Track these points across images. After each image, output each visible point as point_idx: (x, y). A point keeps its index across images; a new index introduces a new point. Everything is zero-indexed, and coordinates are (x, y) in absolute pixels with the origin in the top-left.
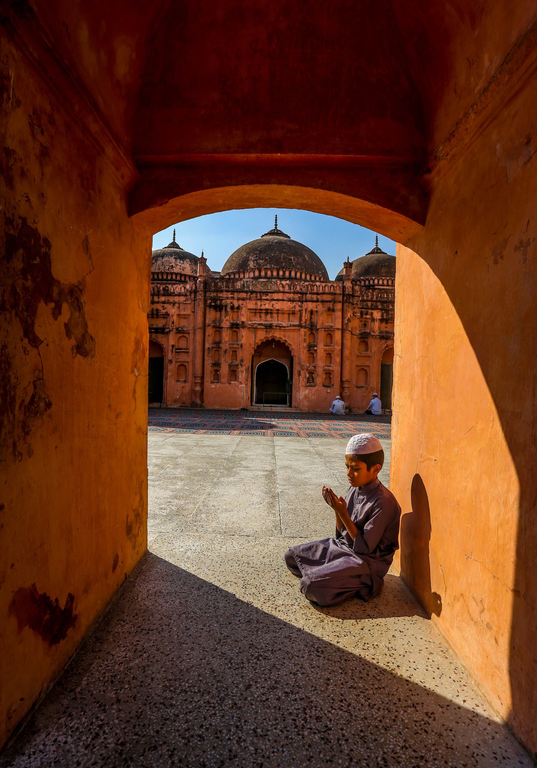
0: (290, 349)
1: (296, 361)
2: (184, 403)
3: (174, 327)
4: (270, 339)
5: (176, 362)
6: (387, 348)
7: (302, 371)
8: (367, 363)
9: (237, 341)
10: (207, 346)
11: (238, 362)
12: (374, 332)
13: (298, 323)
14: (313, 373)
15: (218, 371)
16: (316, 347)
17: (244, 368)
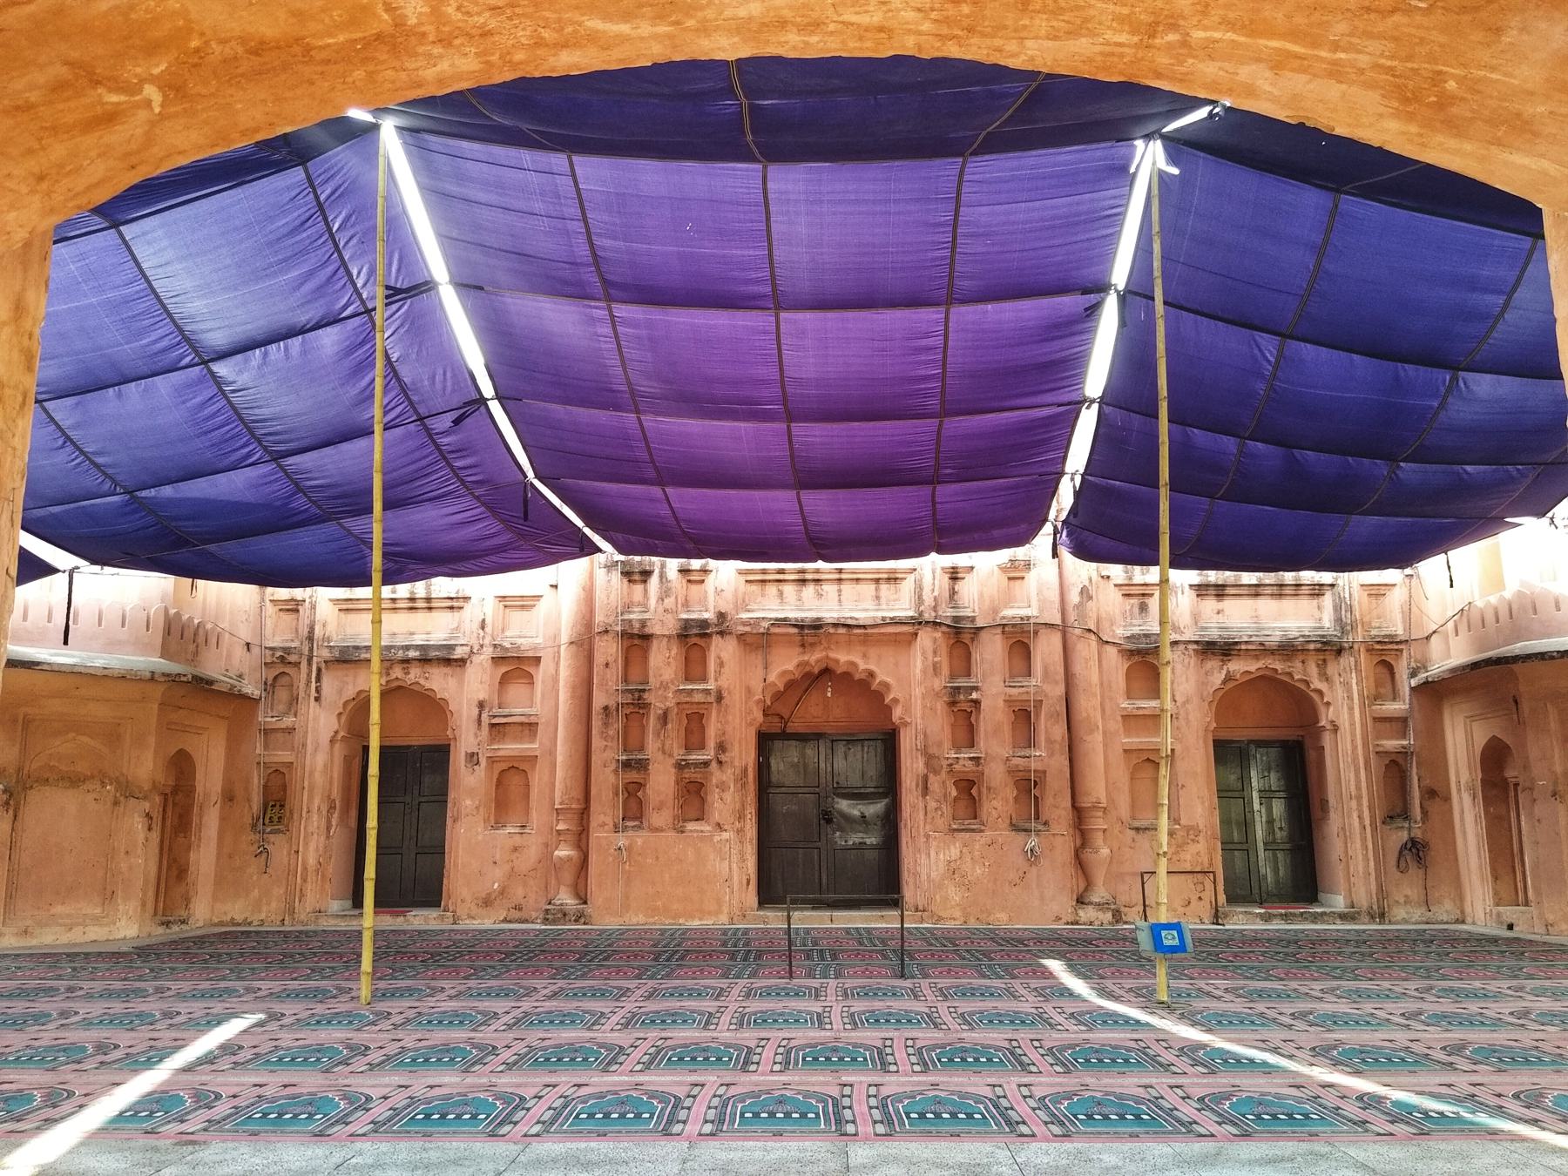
1: (907, 742)
2: (518, 908)
3: (487, 641)
4: (816, 671)
5: (492, 761)
6: (1231, 685)
7: (932, 777)
9: (704, 679)
10: (599, 700)
11: (708, 754)
13: (911, 613)
15: (641, 785)
16: (976, 689)
17: (727, 775)
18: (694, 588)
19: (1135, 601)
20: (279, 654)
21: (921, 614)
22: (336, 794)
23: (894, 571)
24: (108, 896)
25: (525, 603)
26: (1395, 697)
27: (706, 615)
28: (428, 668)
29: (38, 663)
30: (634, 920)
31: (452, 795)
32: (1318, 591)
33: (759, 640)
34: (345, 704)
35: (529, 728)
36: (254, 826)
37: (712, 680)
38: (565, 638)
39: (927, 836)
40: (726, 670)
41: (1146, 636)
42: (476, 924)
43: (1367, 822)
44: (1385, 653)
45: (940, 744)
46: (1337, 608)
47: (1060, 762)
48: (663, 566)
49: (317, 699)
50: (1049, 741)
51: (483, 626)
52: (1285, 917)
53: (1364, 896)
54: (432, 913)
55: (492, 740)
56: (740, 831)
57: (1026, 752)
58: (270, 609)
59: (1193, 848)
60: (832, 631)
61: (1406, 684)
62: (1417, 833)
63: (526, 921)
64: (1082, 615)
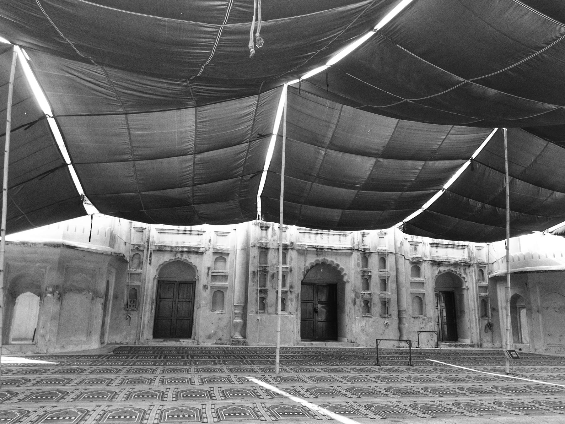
2: (220, 339)
3: (211, 246)
6: (440, 274)
7: (357, 300)
8: (421, 290)
10: (251, 269)
12: (425, 256)
13: (351, 246)
14: (368, 302)
16: (370, 272)
18: (283, 233)
19: (413, 247)
20: (136, 247)
22: (154, 297)
24: (89, 334)
26: (483, 280)
27: (287, 243)
28: (190, 255)
29: (77, 247)
30: (262, 344)
31: (196, 299)
32: (464, 247)
33: (303, 252)
34: (160, 265)
35: (225, 277)
36: (125, 308)
37: (288, 264)
39: (355, 318)
40: (293, 261)
42: (205, 345)
43: (477, 318)
44: (482, 267)
45: (359, 289)
46: (469, 253)
47: (394, 297)
48: (273, 225)
49: (150, 264)
50: (392, 290)
52: (455, 346)
53: (476, 340)
55: (212, 280)
56: (297, 315)
57: (384, 292)
58: (133, 231)
59: (431, 324)
60: (326, 250)
61: (487, 277)
62: (490, 321)
63: (223, 344)
64: (401, 251)
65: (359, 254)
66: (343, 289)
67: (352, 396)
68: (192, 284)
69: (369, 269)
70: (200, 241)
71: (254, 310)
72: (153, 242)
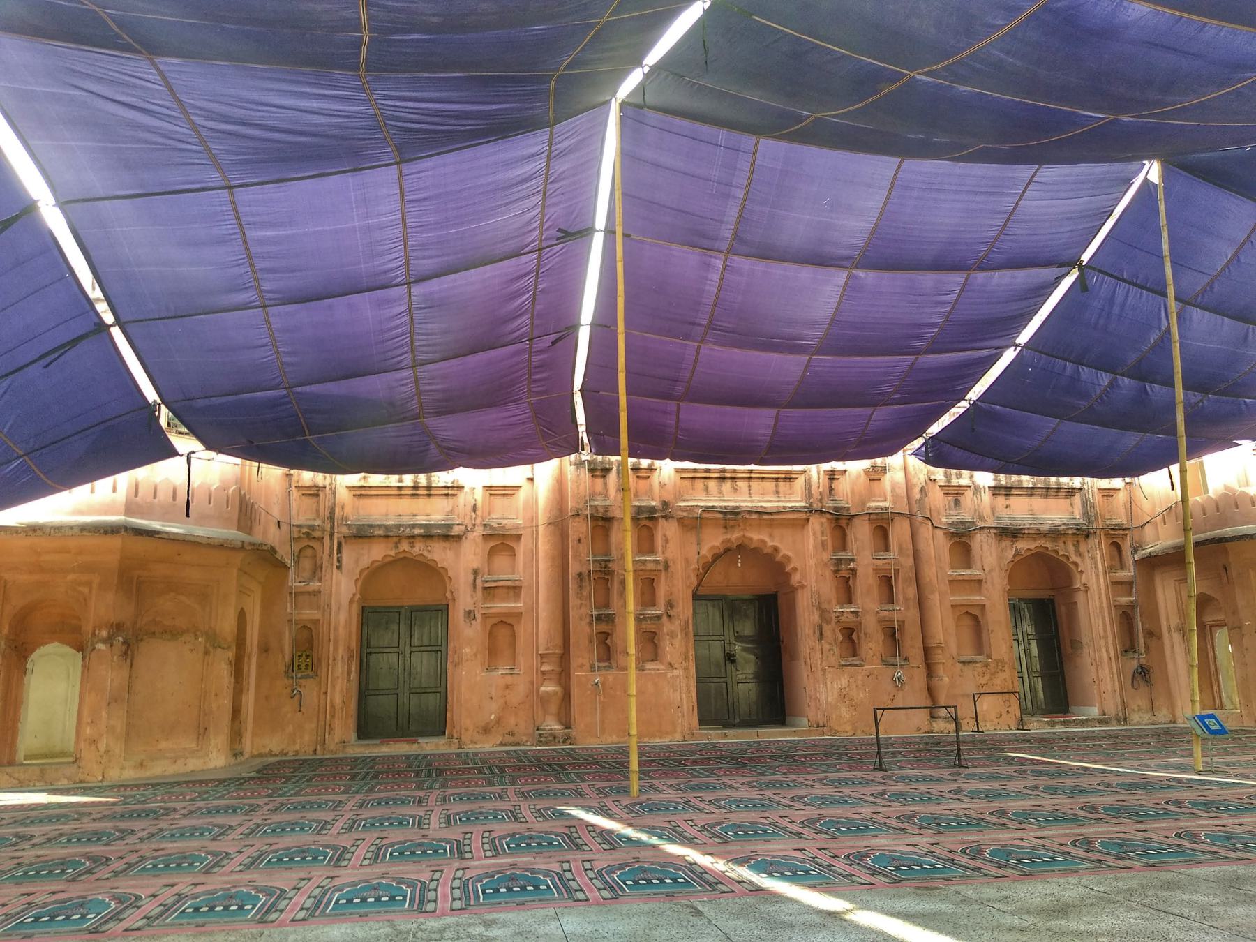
0: (788, 569)
1: (804, 602)
2: (511, 734)
3: (478, 521)
6: (1018, 558)
7: (826, 628)
10: (574, 568)
12: (981, 518)
13: (803, 504)
14: (852, 631)
16: (853, 560)
17: (675, 626)
18: (642, 482)
19: (951, 498)
20: (304, 530)
21: (811, 505)
22: (354, 645)
23: (790, 472)
24: (202, 732)
25: (507, 492)
26: (1122, 567)
27: (653, 504)
28: (429, 542)
29: (159, 532)
30: (609, 740)
32: (1071, 492)
33: (693, 523)
34: (361, 572)
35: (515, 590)
36: (287, 673)
38: (542, 518)
39: (824, 670)
40: (670, 545)
41: (962, 523)
42: (478, 747)
43: (1112, 655)
44: (1116, 537)
45: (829, 602)
46: (1084, 505)
47: (913, 614)
49: (338, 568)
50: (906, 599)
51: (474, 509)
52: (1064, 723)
53: (1112, 707)
54: (442, 741)
55: (485, 600)
56: (686, 669)
57: (890, 607)
58: (295, 494)
59: (1002, 676)
61: (1130, 559)
62: (1143, 662)
64: (922, 508)
65: (824, 520)
66: (792, 607)
67: (815, 836)
68: (440, 611)
69: (849, 555)
70: (452, 512)
71: (586, 662)
72: (344, 518)
